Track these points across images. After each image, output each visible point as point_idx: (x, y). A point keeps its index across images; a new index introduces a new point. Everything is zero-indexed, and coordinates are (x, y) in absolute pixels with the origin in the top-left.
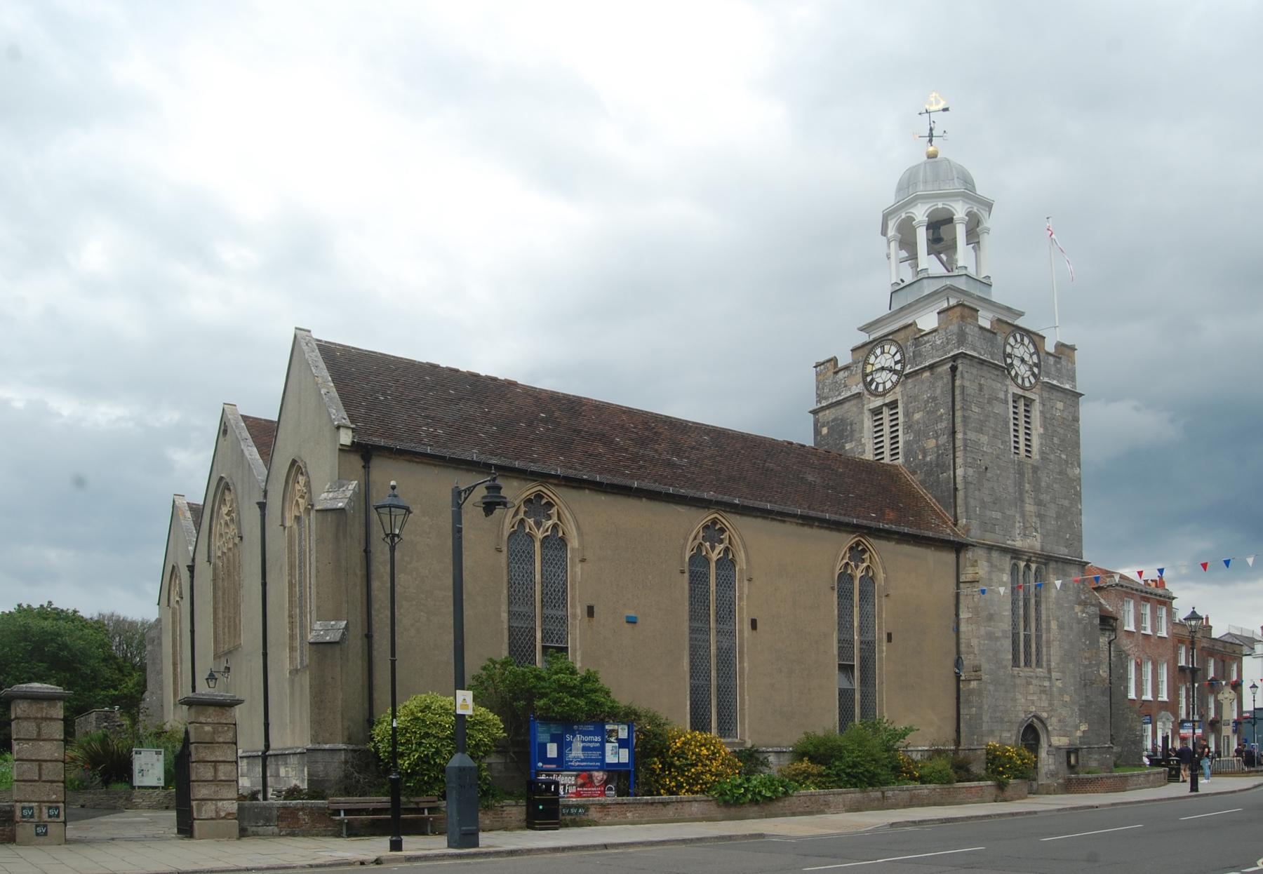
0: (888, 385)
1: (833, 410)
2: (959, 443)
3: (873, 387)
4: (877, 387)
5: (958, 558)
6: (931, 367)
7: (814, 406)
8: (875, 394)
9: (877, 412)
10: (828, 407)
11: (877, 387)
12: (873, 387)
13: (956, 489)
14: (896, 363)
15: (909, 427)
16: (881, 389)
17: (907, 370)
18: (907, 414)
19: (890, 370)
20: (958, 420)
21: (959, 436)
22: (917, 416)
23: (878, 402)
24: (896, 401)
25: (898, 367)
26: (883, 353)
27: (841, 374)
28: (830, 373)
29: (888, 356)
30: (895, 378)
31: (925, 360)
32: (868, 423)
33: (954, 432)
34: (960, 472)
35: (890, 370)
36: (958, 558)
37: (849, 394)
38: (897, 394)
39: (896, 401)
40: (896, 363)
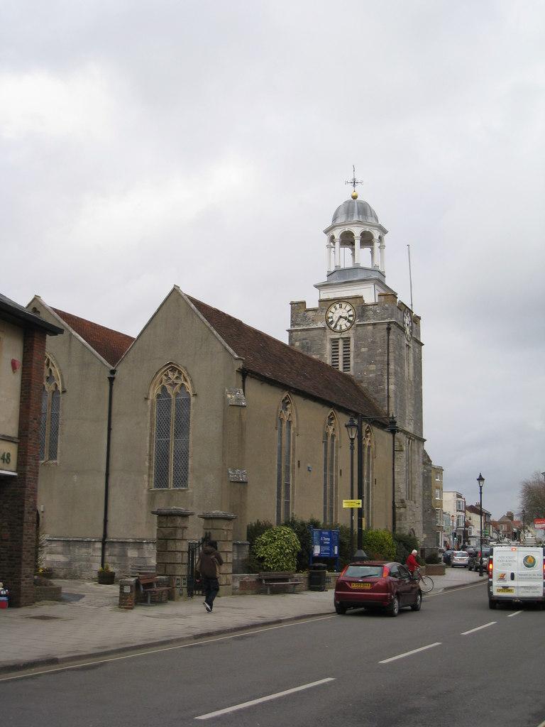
0: (344, 327)
1: (304, 333)
2: (390, 371)
3: (333, 326)
4: (336, 326)
5: (394, 437)
6: (374, 324)
7: (289, 328)
8: (334, 330)
9: (335, 341)
10: (300, 330)
11: (336, 326)
12: (333, 326)
13: (388, 396)
14: (350, 316)
15: (357, 355)
16: (338, 328)
17: (357, 322)
18: (356, 346)
19: (346, 318)
20: (391, 357)
21: (392, 367)
22: (363, 350)
23: (337, 336)
24: (349, 338)
25: (351, 318)
26: (341, 307)
27: (310, 313)
28: (302, 311)
29: (344, 311)
30: (349, 324)
31: (369, 318)
32: (328, 347)
33: (388, 364)
34: (392, 387)
35: (346, 318)
36: (394, 437)
37: (315, 326)
38: (351, 334)
39: (349, 338)
40: (350, 316)
